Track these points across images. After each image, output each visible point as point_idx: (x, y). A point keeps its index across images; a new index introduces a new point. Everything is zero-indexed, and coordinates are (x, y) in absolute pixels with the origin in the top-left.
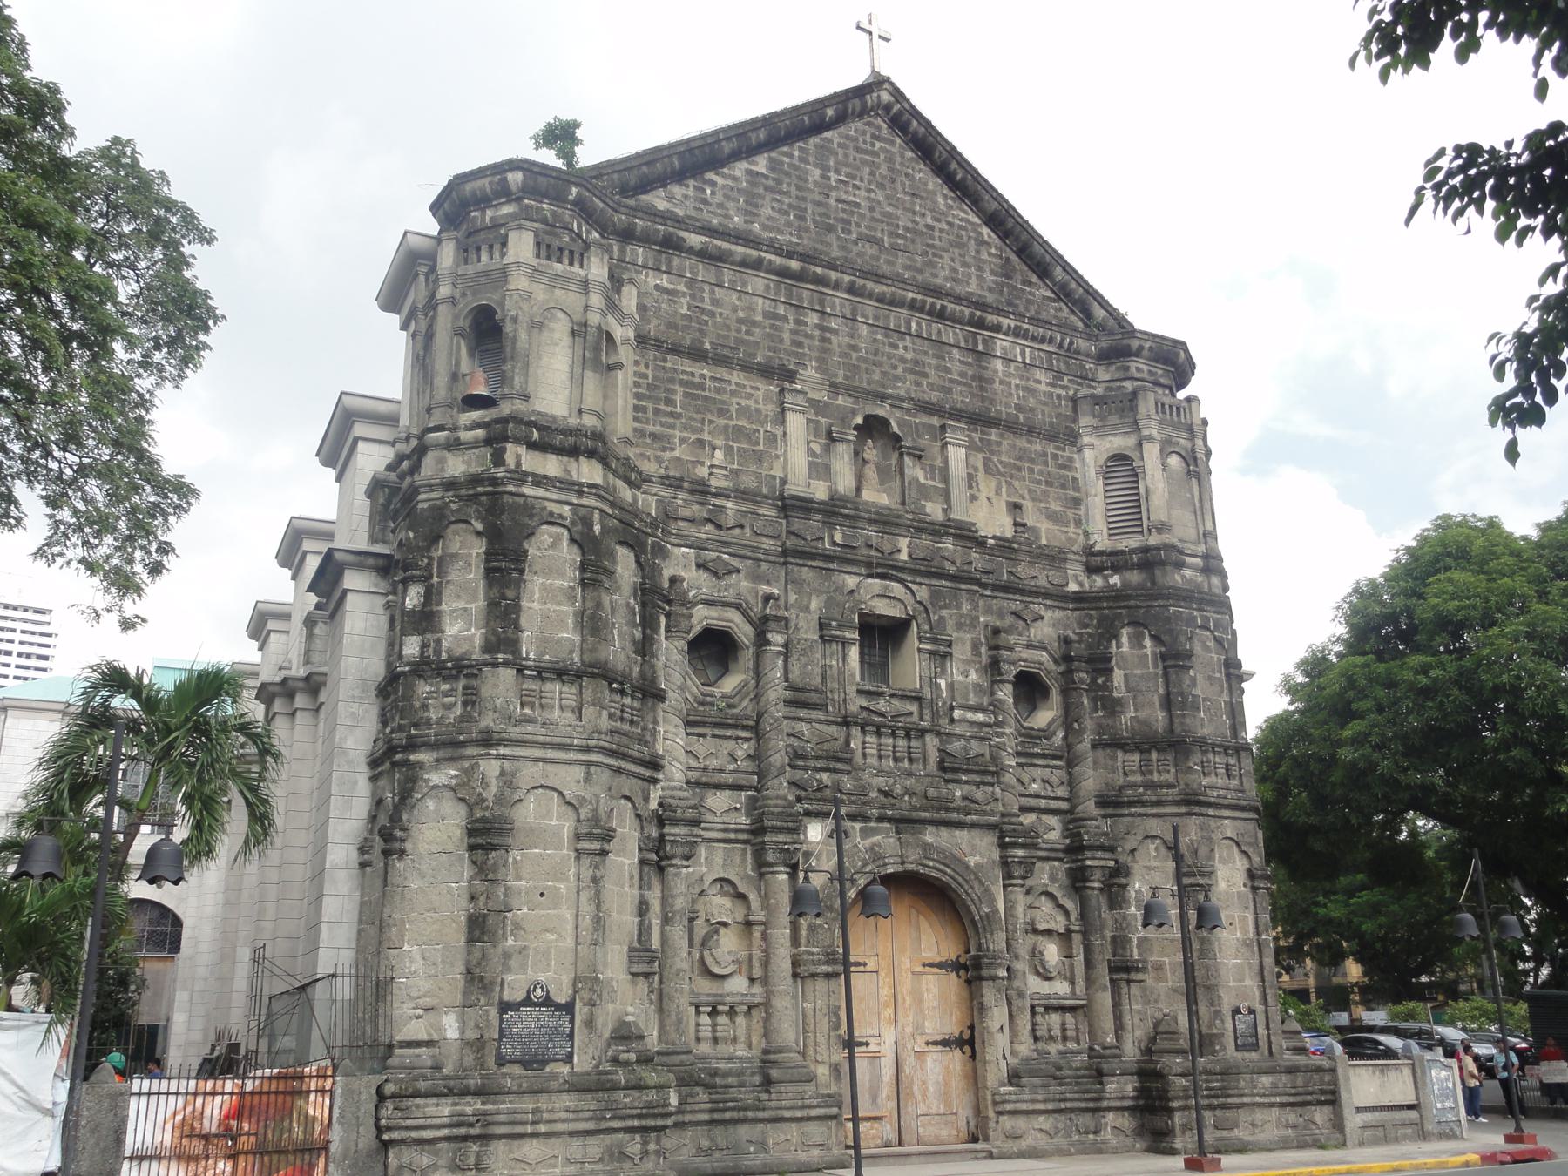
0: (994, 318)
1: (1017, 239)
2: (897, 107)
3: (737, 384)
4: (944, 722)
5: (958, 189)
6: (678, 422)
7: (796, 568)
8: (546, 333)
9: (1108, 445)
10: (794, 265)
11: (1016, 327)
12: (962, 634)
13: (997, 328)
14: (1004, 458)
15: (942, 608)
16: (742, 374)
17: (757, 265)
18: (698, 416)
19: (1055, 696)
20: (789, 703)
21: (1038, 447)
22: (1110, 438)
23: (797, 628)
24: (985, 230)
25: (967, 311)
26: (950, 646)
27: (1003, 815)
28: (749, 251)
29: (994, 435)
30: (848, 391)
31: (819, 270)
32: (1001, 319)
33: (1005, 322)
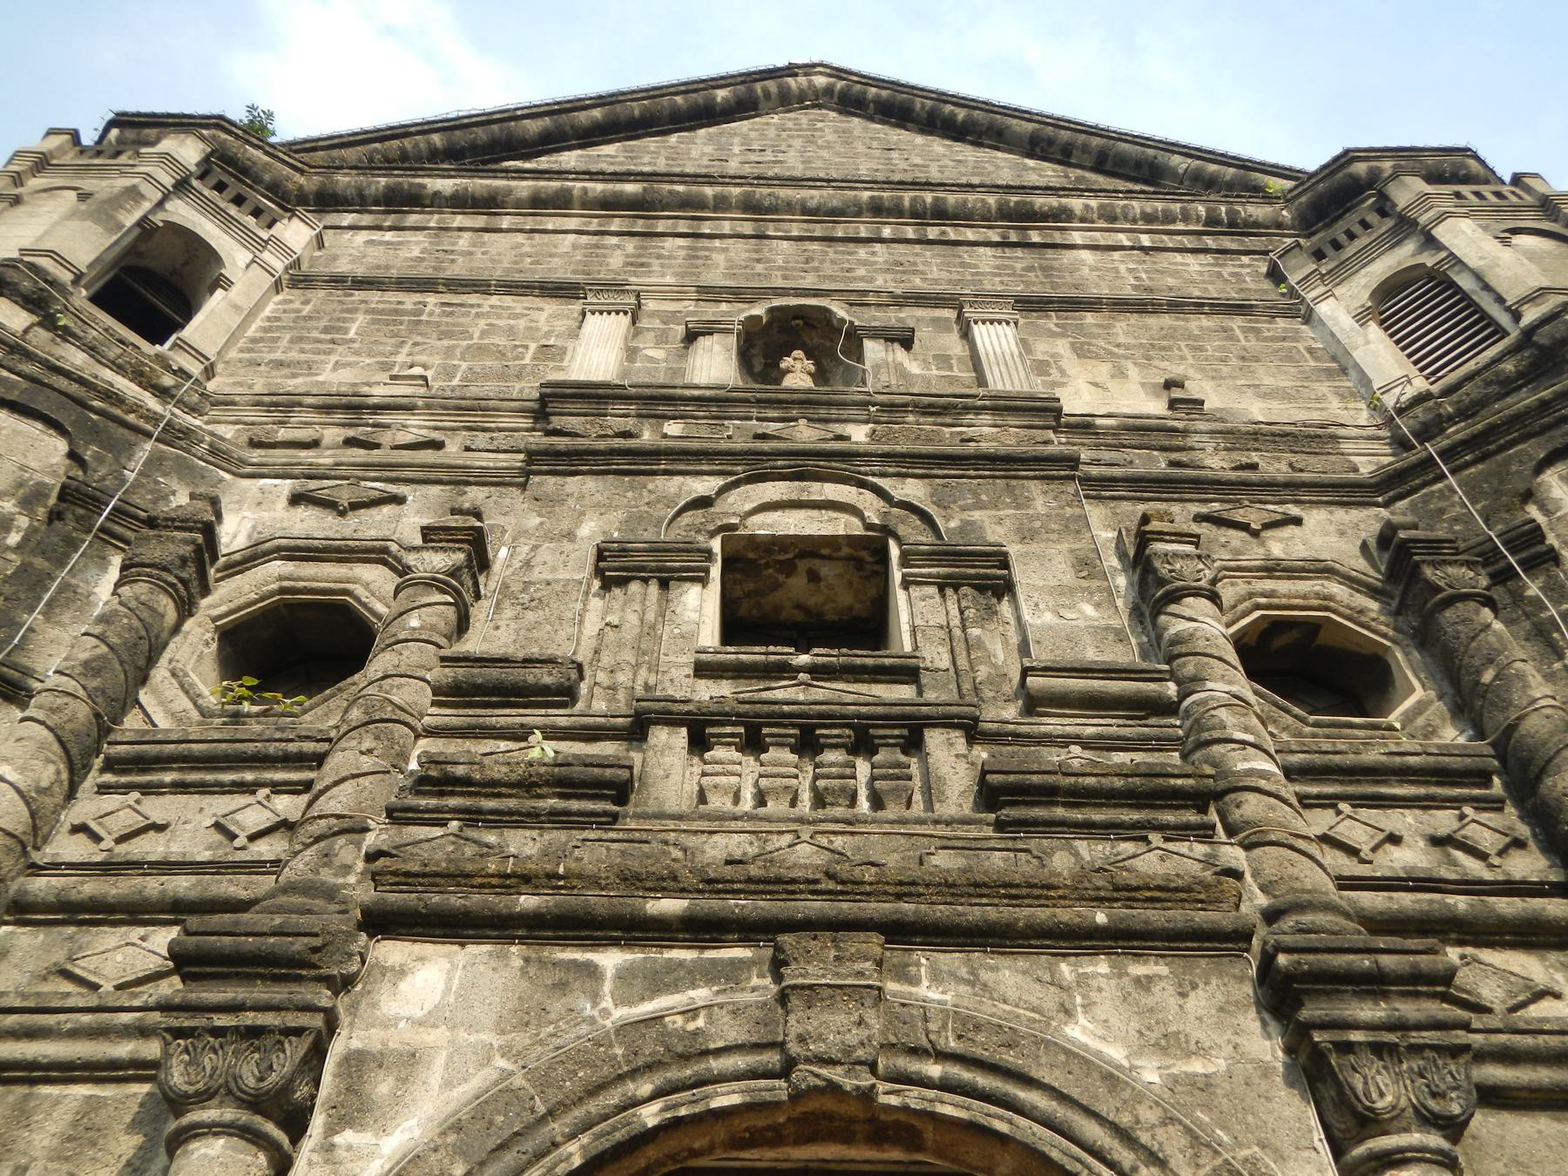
0: (1054, 201)
1: (1085, 148)
2: (840, 84)
3: (491, 307)
4: (1011, 712)
5: (969, 133)
6: (340, 349)
7: (551, 480)
8: (21, 209)
9: (1363, 281)
10: (630, 188)
11: (1101, 207)
12: (1034, 547)
13: (1063, 215)
14: (1122, 340)
15: (963, 509)
16: (508, 298)
17: (561, 202)
18: (393, 340)
19: (1405, 663)
20: (449, 694)
21: (1205, 322)
22: (1363, 271)
23: (527, 564)
24: (1031, 163)
25: (991, 200)
26: (1005, 565)
27: (1271, 916)
28: (542, 183)
29: (1090, 318)
30: (738, 295)
31: (680, 188)
32: (1064, 200)
33: (1076, 204)
